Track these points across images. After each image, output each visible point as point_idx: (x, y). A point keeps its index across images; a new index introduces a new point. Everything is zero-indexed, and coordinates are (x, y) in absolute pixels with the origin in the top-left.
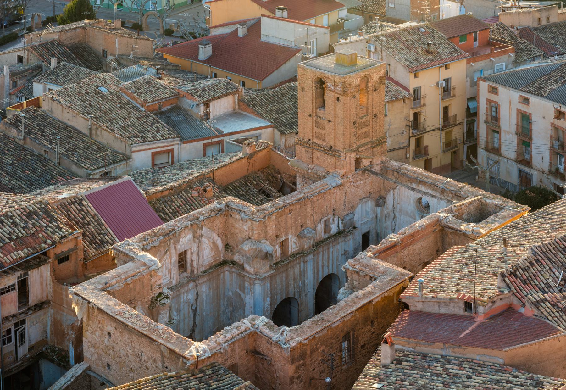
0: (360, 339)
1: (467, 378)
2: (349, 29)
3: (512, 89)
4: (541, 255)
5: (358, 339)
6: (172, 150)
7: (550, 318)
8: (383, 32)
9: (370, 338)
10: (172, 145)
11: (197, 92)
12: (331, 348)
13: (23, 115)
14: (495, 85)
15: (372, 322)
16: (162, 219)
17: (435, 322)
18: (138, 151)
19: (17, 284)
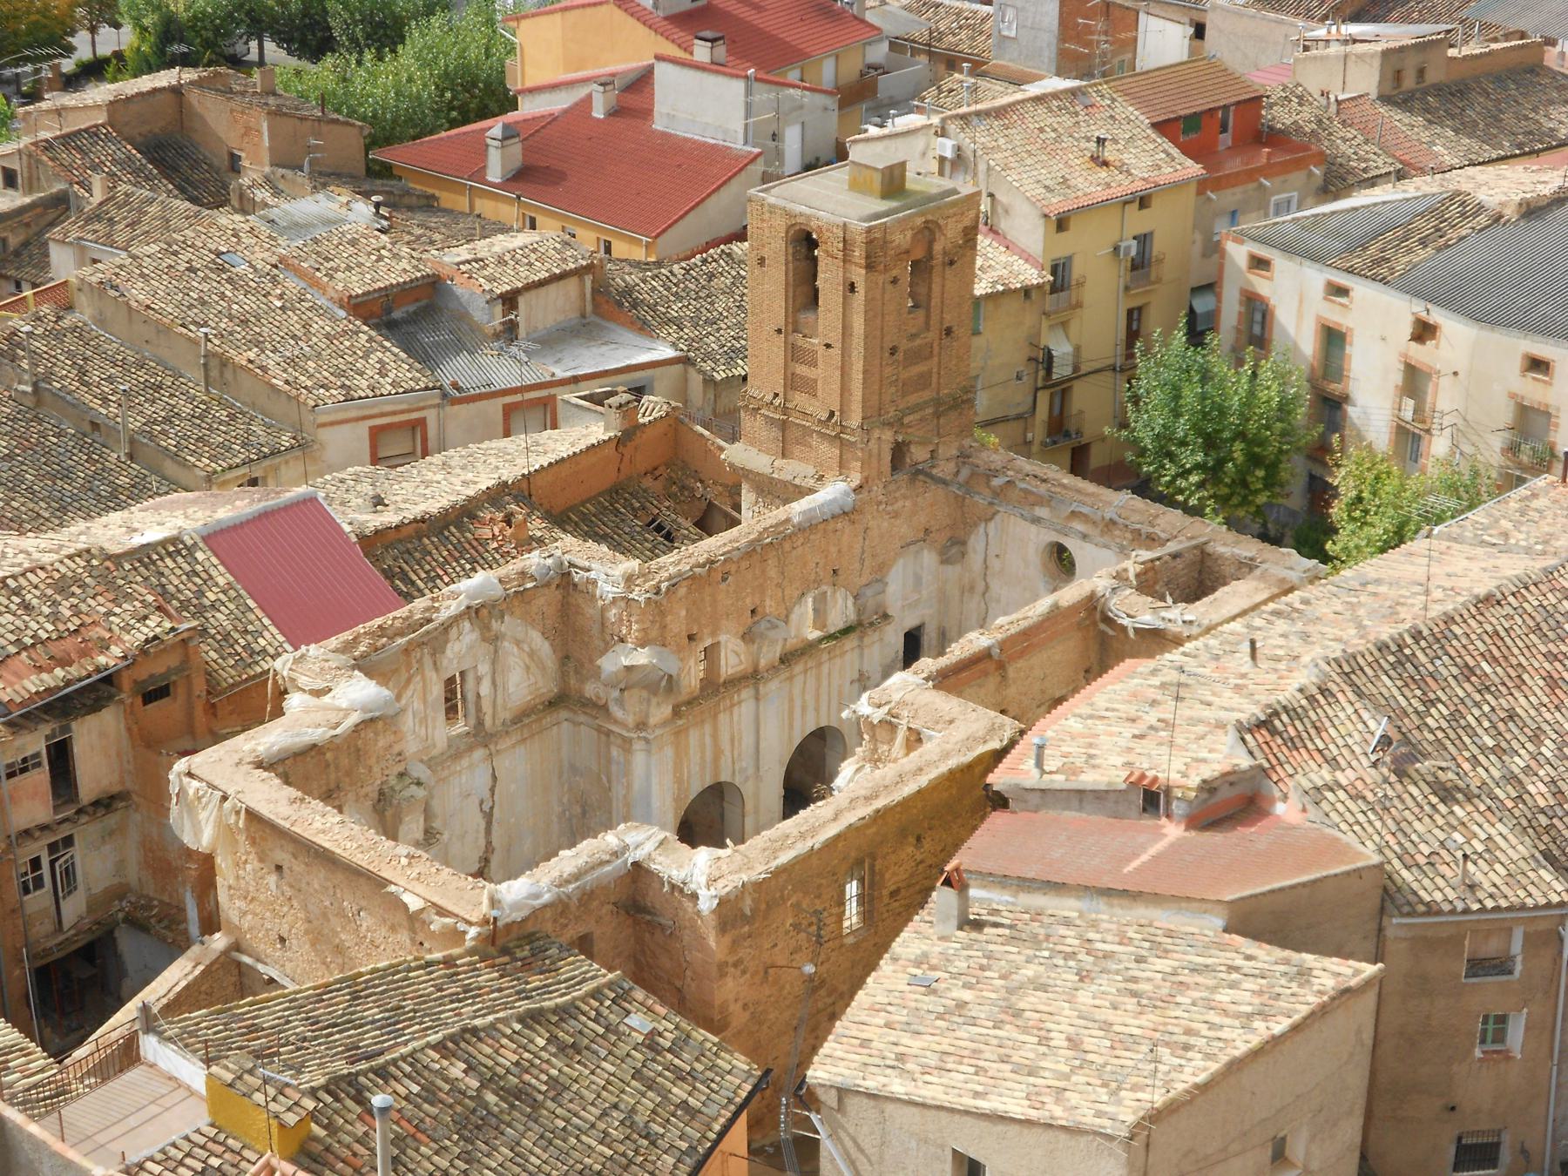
0: (887, 876)
1: (1137, 961)
2: (891, 97)
3: (1308, 263)
4: (1338, 680)
5: (882, 876)
6: (422, 422)
7: (1344, 826)
8: (979, 107)
9: (912, 876)
10: (422, 408)
11: (483, 268)
12: (818, 897)
13: (27, 328)
14: (1263, 252)
15: (919, 839)
16: (400, 593)
17: (1069, 838)
18: (332, 424)
19: (44, 752)
